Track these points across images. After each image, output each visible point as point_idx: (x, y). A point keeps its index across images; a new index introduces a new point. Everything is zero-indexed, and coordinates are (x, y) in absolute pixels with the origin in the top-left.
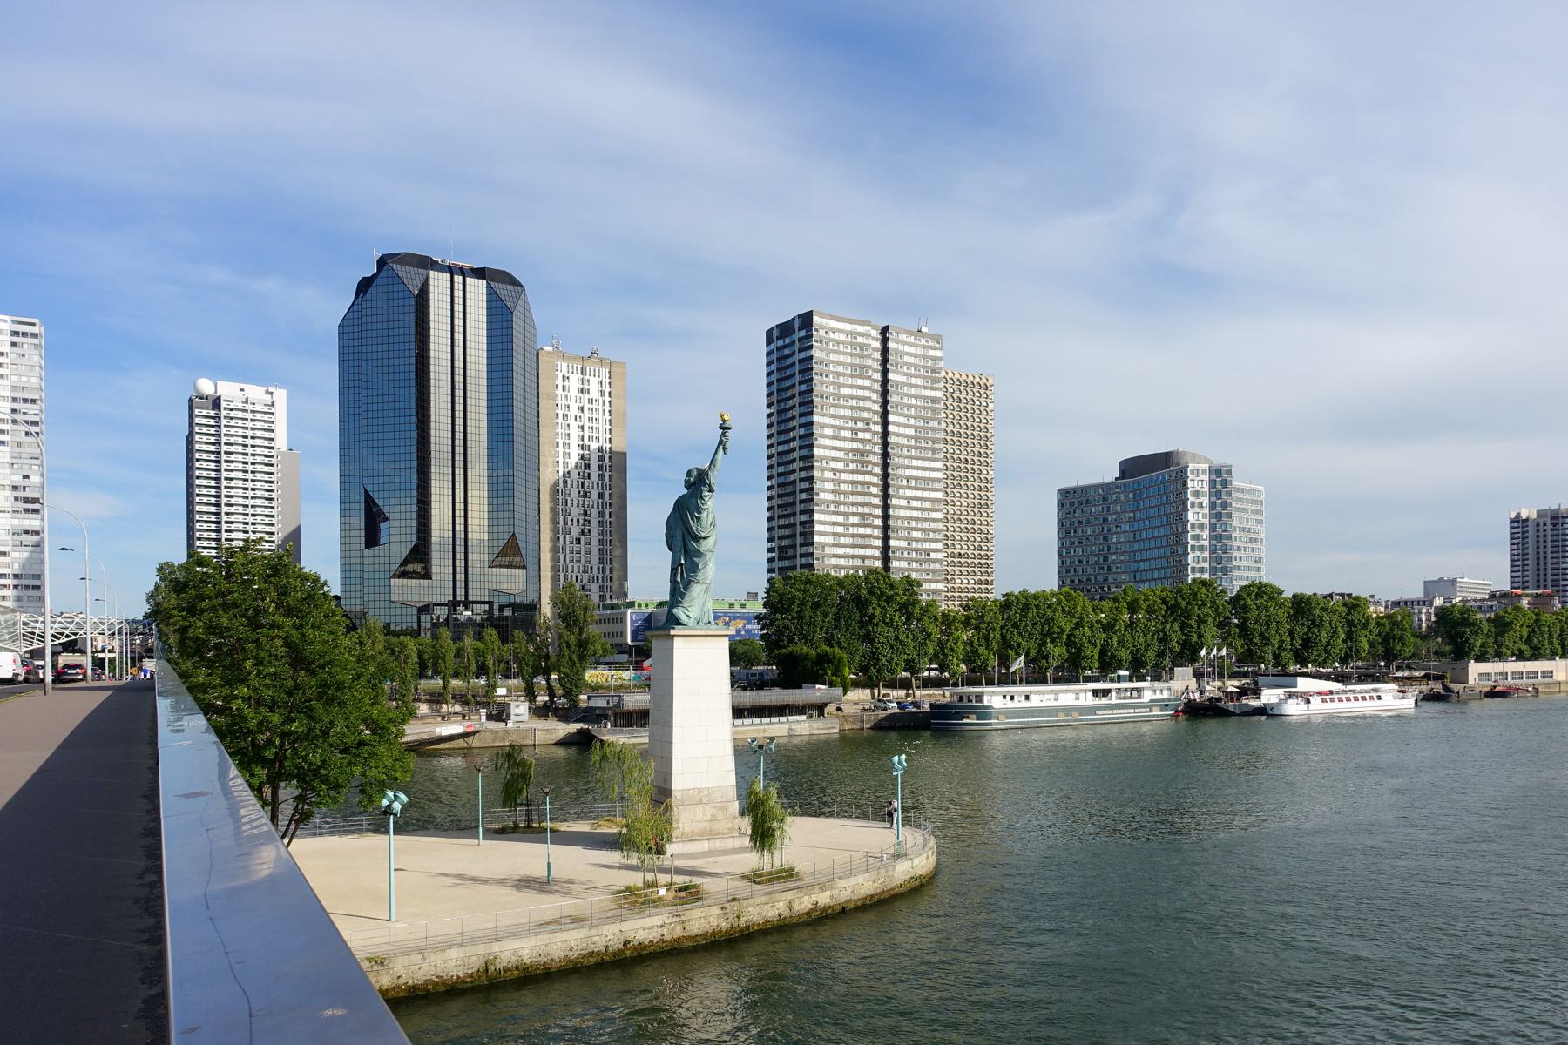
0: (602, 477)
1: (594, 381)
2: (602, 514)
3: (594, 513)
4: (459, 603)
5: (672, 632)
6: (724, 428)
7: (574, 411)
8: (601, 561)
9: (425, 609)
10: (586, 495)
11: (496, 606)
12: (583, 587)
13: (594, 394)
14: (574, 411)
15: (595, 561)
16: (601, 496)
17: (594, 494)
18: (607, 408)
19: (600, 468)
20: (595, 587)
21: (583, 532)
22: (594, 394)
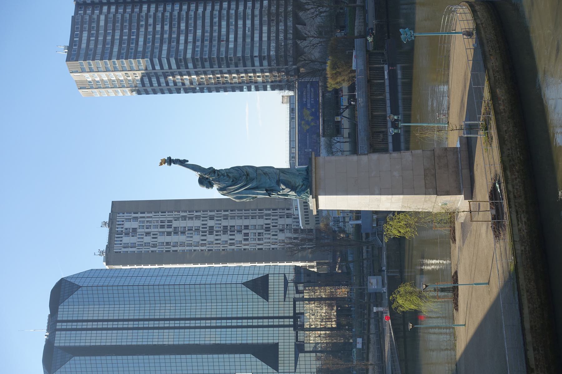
0: (197, 217)
1: (127, 225)
2: (226, 218)
3: (225, 223)
4: (294, 322)
5: (315, 213)
6: (170, 161)
7: (147, 239)
8: (261, 217)
9: (300, 348)
10: (211, 228)
11: (297, 296)
12: (282, 231)
13: (135, 225)
14: (147, 239)
15: (261, 222)
16: (212, 218)
17: (211, 223)
18: (146, 215)
19: (191, 218)
20: (281, 222)
21: (240, 231)
22: (135, 225)
